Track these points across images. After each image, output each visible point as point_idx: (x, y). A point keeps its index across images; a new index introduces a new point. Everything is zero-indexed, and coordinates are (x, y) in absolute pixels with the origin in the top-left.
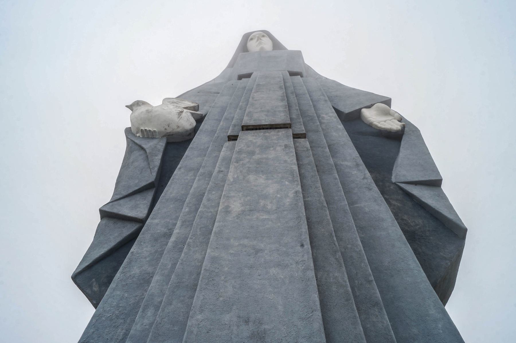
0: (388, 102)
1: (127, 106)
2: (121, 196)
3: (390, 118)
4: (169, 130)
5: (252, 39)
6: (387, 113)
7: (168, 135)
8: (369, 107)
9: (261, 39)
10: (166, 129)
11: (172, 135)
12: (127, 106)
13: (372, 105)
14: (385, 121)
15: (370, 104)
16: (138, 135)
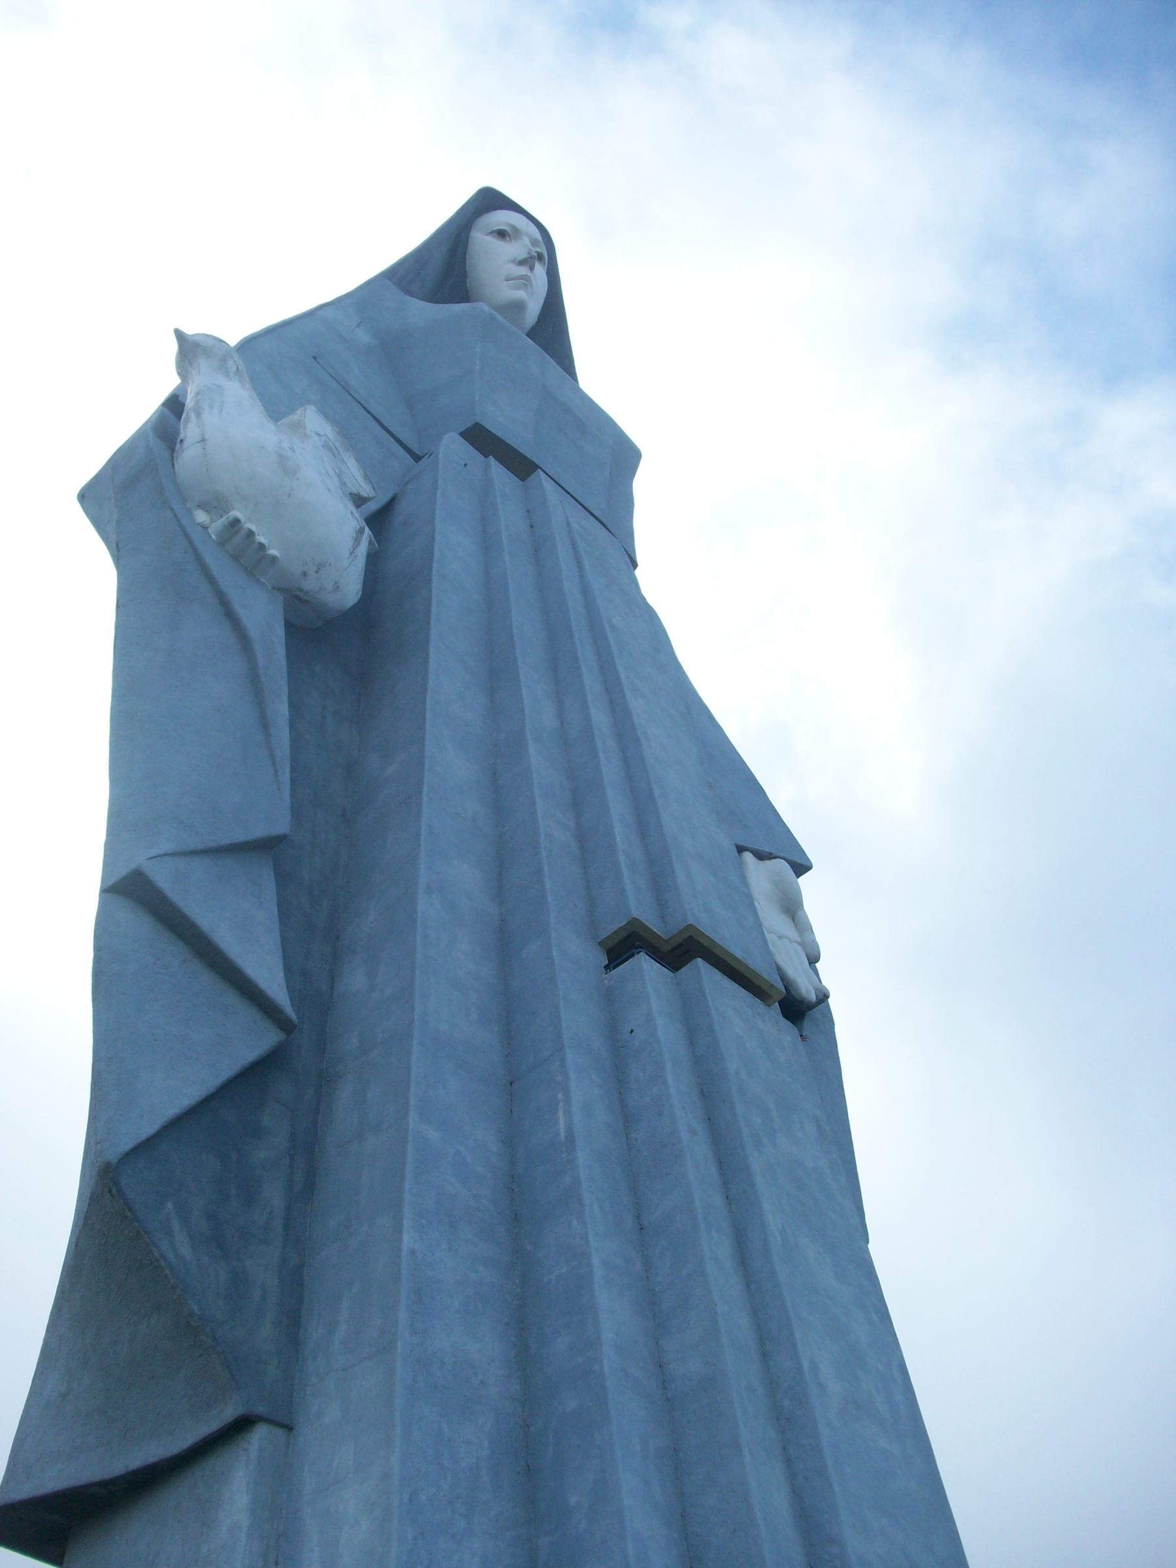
0: (801, 867)
1: (179, 335)
2: (200, 846)
3: (794, 935)
4: (310, 585)
5: (502, 234)
6: (792, 907)
7: (297, 597)
8: (761, 856)
9: (532, 268)
10: (305, 574)
11: (307, 602)
12: (179, 335)
13: (770, 856)
14: (781, 937)
15: (767, 849)
16: (201, 517)
